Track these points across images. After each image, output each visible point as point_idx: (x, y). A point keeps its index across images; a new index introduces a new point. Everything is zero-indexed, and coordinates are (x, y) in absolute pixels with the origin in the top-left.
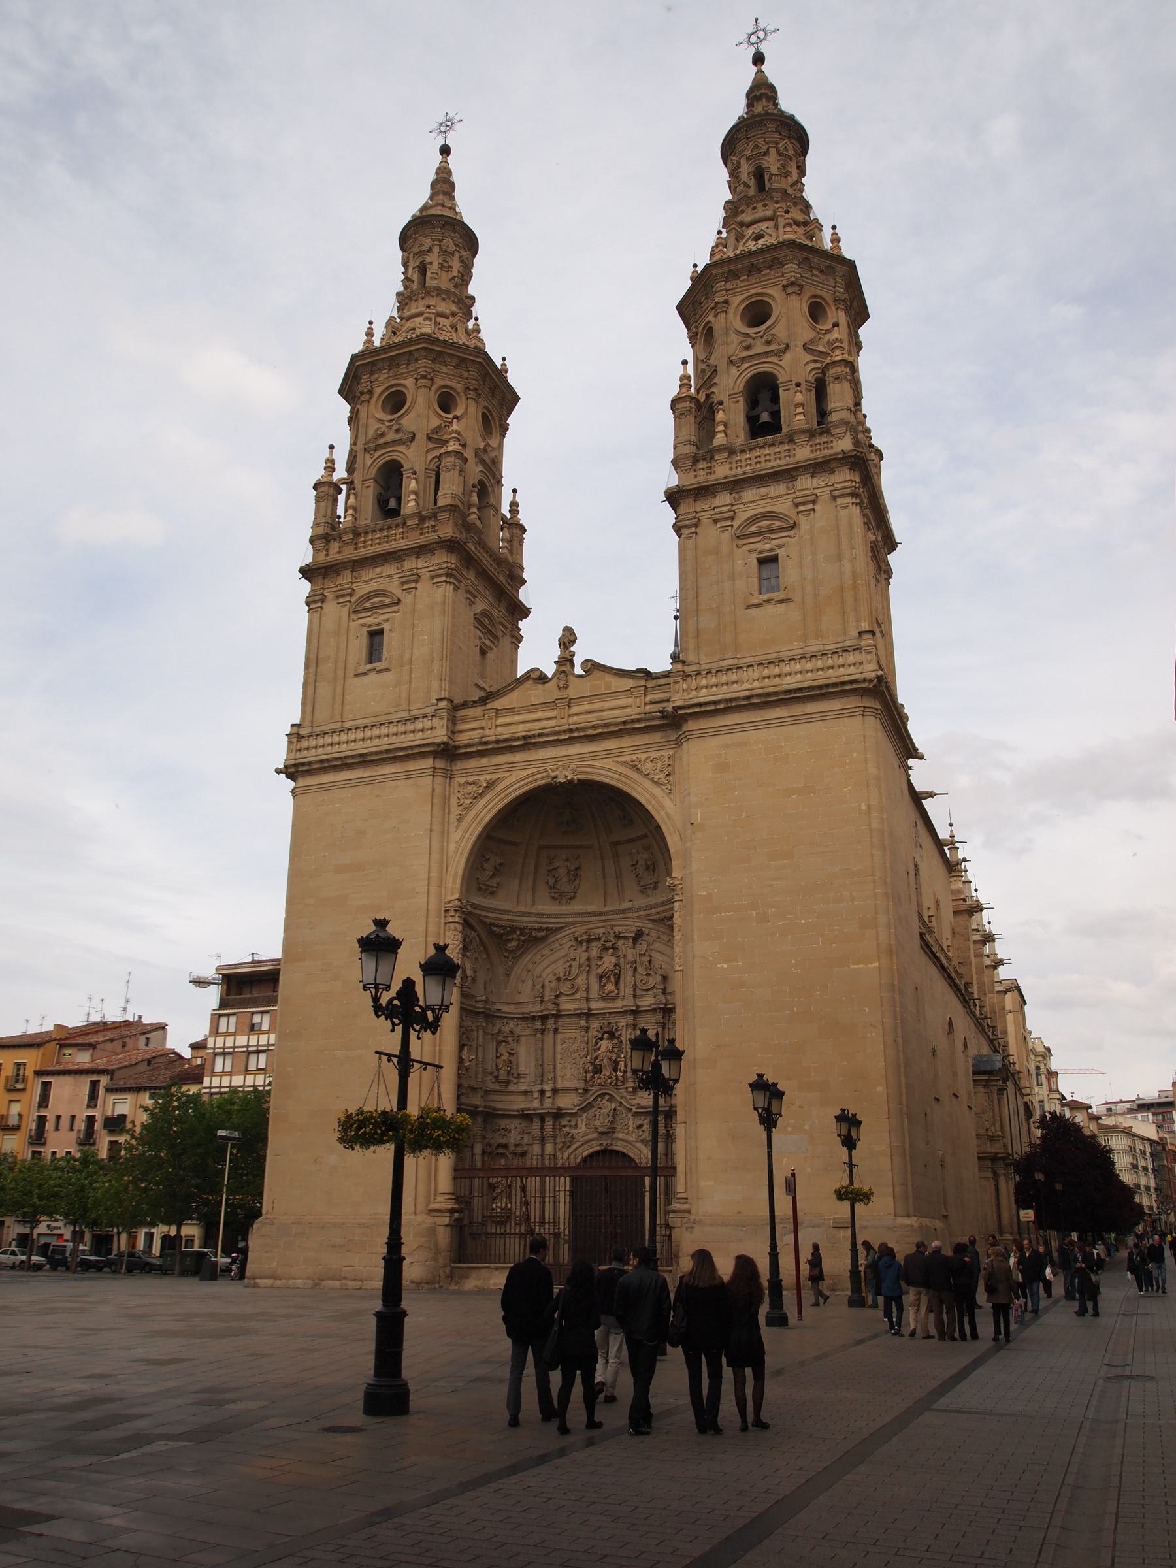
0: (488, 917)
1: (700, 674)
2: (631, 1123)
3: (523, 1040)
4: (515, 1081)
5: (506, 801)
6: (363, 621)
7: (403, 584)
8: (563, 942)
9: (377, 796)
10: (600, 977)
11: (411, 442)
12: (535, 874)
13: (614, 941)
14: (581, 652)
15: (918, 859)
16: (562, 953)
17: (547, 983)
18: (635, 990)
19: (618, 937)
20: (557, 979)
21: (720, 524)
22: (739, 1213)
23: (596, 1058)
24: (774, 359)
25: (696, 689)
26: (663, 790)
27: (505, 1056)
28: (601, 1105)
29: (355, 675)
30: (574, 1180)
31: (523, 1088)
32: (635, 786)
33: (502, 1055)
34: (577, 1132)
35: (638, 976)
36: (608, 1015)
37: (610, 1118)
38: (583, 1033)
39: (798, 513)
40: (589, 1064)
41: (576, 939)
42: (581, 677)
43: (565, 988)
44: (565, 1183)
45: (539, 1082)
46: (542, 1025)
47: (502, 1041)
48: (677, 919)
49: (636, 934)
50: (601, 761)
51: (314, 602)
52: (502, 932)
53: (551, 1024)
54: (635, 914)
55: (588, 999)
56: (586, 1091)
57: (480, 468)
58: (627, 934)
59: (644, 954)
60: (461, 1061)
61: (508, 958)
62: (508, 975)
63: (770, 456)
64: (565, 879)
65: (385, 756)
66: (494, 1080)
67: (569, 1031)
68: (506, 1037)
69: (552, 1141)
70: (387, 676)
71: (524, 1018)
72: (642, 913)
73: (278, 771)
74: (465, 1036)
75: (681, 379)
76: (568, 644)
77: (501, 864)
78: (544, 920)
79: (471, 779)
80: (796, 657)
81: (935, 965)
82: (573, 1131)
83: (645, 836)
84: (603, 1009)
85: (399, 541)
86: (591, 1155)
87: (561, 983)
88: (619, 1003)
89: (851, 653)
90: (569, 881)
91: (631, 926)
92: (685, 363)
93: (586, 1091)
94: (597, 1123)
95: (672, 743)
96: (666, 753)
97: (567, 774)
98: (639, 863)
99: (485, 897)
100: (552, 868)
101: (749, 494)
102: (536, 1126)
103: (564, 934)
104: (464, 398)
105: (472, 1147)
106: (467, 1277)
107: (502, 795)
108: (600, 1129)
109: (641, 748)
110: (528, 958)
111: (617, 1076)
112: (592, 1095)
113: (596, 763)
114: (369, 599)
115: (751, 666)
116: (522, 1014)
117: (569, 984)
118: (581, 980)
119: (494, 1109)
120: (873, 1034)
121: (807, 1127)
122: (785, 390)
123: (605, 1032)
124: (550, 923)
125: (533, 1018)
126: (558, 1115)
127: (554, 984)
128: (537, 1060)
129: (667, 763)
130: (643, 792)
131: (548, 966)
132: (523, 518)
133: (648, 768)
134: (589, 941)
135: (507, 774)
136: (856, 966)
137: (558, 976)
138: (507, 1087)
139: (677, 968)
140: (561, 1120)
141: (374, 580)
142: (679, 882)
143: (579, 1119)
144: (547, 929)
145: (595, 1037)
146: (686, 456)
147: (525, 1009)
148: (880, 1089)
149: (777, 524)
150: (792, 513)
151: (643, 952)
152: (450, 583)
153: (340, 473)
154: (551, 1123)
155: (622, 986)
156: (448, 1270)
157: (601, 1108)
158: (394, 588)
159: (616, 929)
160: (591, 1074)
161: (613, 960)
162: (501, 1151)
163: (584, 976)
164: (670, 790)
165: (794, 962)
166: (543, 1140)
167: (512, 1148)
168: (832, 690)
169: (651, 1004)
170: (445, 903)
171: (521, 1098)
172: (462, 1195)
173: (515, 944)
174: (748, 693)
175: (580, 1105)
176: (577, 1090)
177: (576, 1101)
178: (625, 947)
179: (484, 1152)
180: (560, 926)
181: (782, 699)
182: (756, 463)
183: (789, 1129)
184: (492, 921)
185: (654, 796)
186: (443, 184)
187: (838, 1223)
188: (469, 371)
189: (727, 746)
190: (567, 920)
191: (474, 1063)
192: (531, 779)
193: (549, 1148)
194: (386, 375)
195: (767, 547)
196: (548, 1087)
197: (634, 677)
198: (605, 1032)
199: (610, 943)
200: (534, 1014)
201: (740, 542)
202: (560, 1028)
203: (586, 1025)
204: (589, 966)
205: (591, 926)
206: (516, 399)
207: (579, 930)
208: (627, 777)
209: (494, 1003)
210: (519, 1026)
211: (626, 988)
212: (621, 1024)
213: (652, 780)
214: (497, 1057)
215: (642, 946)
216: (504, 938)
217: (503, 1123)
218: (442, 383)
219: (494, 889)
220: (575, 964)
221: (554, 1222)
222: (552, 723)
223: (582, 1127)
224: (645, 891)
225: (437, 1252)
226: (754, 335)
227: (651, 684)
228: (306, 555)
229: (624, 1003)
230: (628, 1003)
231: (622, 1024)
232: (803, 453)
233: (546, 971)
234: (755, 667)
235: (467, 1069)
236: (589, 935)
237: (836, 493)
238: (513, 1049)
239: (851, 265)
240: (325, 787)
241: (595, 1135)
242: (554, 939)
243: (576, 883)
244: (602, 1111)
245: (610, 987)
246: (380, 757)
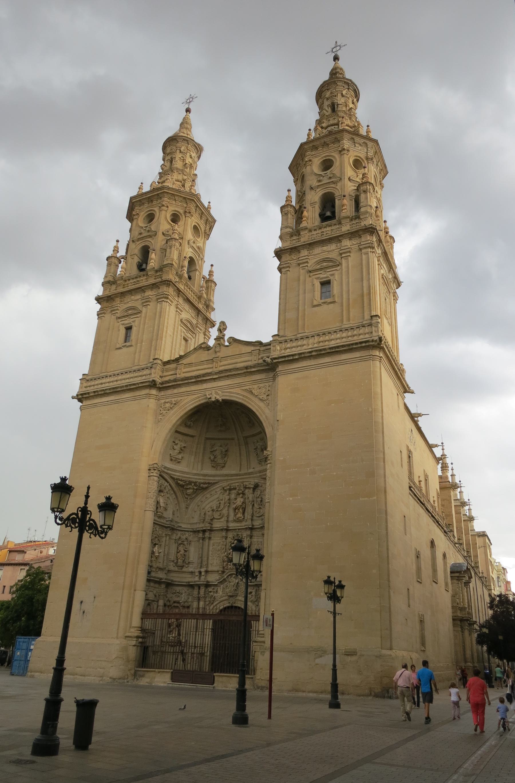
0: (175, 475)
1: (286, 341)
3: (193, 543)
4: (187, 566)
5: (185, 412)
6: (123, 322)
7: (143, 303)
8: (217, 490)
10: (235, 509)
11: (155, 236)
12: (204, 453)
13: (243, 490)
14: (228, 334)
15: (411, 448)
16: (216, 496)
17: (207, 512)
18: (252, 517)
19: (246, 488)
20: (212, 510)
21: (301, 266)
22: (291, 644)
24: (333, 186)
25: (284, 349)
27: (182, 552)
28: (230, 580)
29: (116, 349)
30: (214, 623)
31: (191, 570)
32: (251, 402)
33: (180, 551)
34: (217, 595)
35: (255, 509)
36: (237, 530)
37: (235, 588)
38: (224, 540)
39: (342, 258)
40: (225, 557)
41: (223, 488)
42: (227, 346)
43: (216, 516)
44: (209, 624)
45: (199, 567)
46: (203, 535)
47: (181, 544)
48: (268, 473)
49: (254, 486)
50: (234, 389)
51: (100, 314)
52: (184, 484)
53: (207, 534)
54: (255, 475)
55: (227, 521)
56: (223, 572)
57: (191, 250)
58: (249, 486)
59: (258, 497)
60: (153, 553)
61: (187, 498)
62: (187, 508)
63: (330, 231)
64: (220, 457)
65: (125, 388)
66: (174, 565)
67: (217, 539)
68: (183, 541)
69: (203, 600)
70: (131, 349)
71: (196, 532)
72: (258, 475)
73: (73, 398)
74: (157, 539)
75: (287, 198)
76: (222, 330)
77: (185, 447)
78: (207, 478)
79: (167, 400)
80: (337, 331)
81: (422, 507)
82: (215, 595)
84: (235, 527)
85: (144, 282)
86: (225, 609)
87: (214, 513)
88: (243, 524)
89: (367, 327)
90: (222, 458)
91: (251, 482)
92: (289, 191)
93: (223, 572)
94: (228, 590)
95: (271, 379)
96: (267, 384)
97: (216, 396)
98: (258, 447)
99: (175, 464)
100: (212, 450)
101: (317, 250)
102: (196, 592)
103: (218, 486)
104: (184, 216)
105: (158, 601)
106: (143, 676)
107: (183, 408)
108: (229, 594)
109: (255, 382)
110: (199, 499)
112: (225, 575)
113: (232, 390)
114: (126, 311)
115: (313, 336)
116: (193, 529)
117: (218, 513)
118: (225, 512)
119: (172, 581)
120: (372, 539)
122: (338, 200)
123: (236, 540)
124: (210, 480)
125: (198, 531)
126: (207, 585)
127: (210, 513)
128: (199, 555)
129: (268, 389)
131: (209, 503)
132: (215, 278)
134: (230, 490)
135: (187, 397)
136: (363, 499)
137: (212, 509)
138: (182, 569)
139: (267, 501)
140: (209, 588)
141: (130, 302)
142: (270, 453)
143: (219, 588)
144: (209, 483)
145: (231, 542)
146: (287, 233)
147: (195, 527)
148: (374, 571)
149: (331, 264)
150: (339, 258)
151: (258, 496)
152: (167, 302)
153: (122, 252)
154: (203, 590)
155: (246, 514)
156: (133, 672)
157: (230, 582)
158: (138, 305)
159: (245, 483)
160: (226, 563)
161: (242, 500)
162: (175, 605)
163: (226, 509)
164: (269, 403)
165: (329, 496)
166: (199, 599)
167: (182, 604)
168: (354, 347)
169: (260, 524)
170: (149, 465)
171: (190, 576)
172: (147, 628)
173: (191, 491)
174: (310, 350)
175: (219, 580)
176: (218, 571)
177: (218, 578)
178: (249, 493)
179: (165, 605)
180: (215, 481)
181: (328, 353)
182: (322, 235)
184: (178, 477)
185: (260, 407)
186: (185, 124)
187: (347, 652)
188: (187, 204)
190: (219, 478)
191: (162, 555)
192: (198, 400)
193: (202, 604)
194: (147, 206)
195: (325, 276)
196: (203, 570)
197: (254, 345)
198: (236, 540)
199: (241, 491)
200: (199, 529)
201: (312, 274)
202: (212, 537)
203: (225, 535)
204: (230, 503)
205: (232, 482)
206: (215, 221)
207: (225, 484)
208: (247, 397)
209: (177, 522)
210: (191, 536)
211: (248, 516)
212: (244, 535)
213: (261, 400)
214: (178, 552)
215: (258, 492)
216: (185, 487)
217: (178, 589)
218: (173, 209)
219: (180, 460)
220: (222, 502)
221: (202, 647)
223: (220, 592)
224: (261, 463)
225: (128, 661)
226: (324, 175)
227: (262, 348)
228: (99, 291)
229: (246, 523)
230: (248, 523)
232: (346, 228)
233: (208, 506)
234: (316, 337)
235: (157, 558)
236: (230, 487)
237: (361, 247)
238: (187, 549)
239: (376, 142)
240: (95, 405)
241: (227, 598)
242: (212, 489)
243: (226, 459)
244: (231, 584)
245: (240, 515)
246: (123, 389)
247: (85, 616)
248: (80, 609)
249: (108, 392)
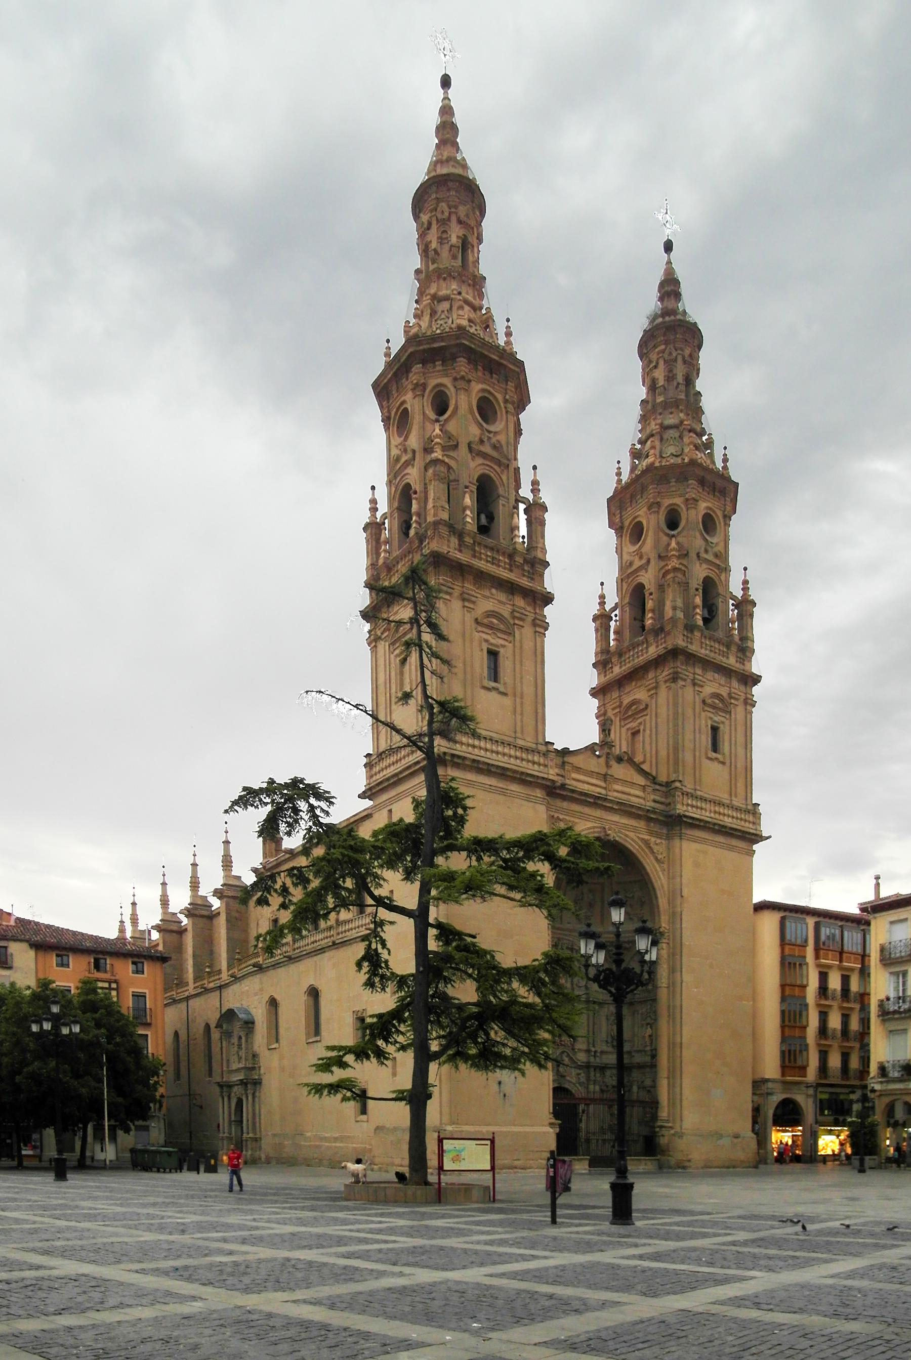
79: (561, 817)
130: (649, 864)
133: (655, 849)
185: (656, 870)
201: (706, 708)
208: (643, 850)
213: (656, 859)
222: (598, 790)
249: (493, 769)
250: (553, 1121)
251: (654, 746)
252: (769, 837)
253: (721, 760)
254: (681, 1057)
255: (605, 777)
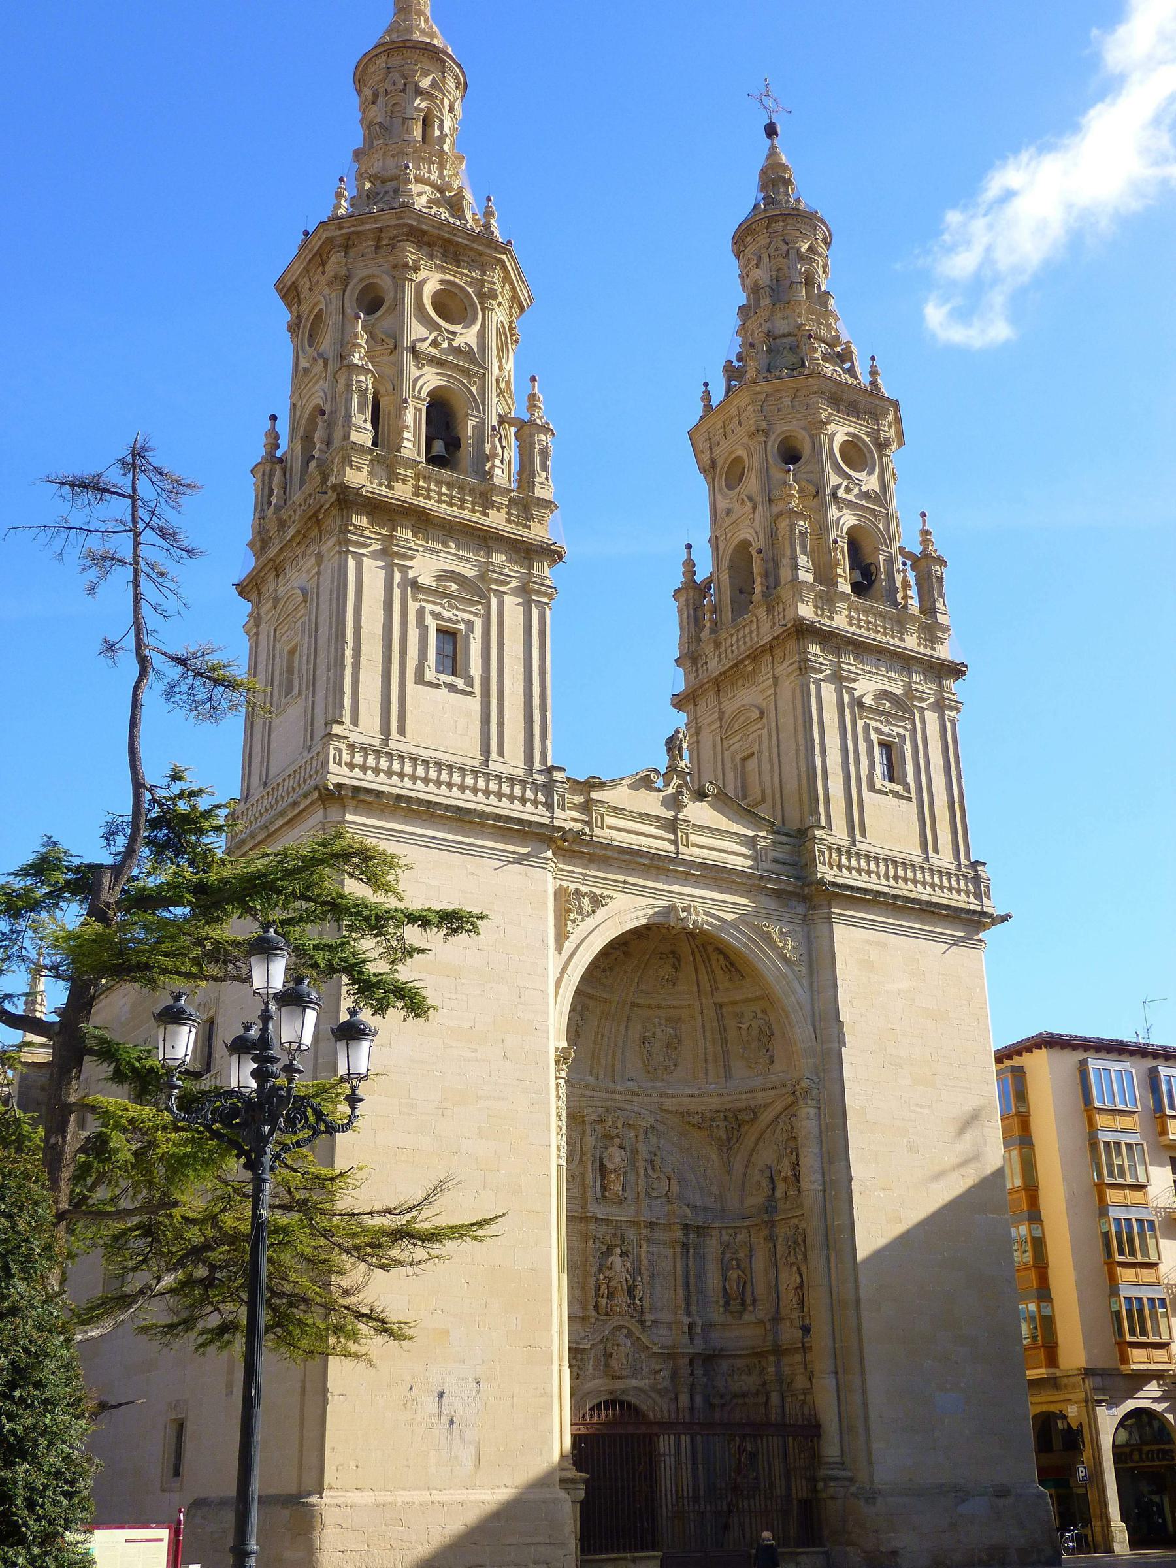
2: (644, 1365)
9: (472, 874)
23: (610, 1279)
26: (793, 970)
79: (584, 889)
83: (688, 1006)
111: (634, 1303)
121: (962, 1385)
183: (948, 1387)
189: (868, 942)
231: (632, 1234)
247: (456, 1432)
248: (440, 1414)
250: (572, 1473)
251: (776, 774)
252: (1005, 918)
253: (902, 792)
254: (859, 1328)
255: (672, 825)
